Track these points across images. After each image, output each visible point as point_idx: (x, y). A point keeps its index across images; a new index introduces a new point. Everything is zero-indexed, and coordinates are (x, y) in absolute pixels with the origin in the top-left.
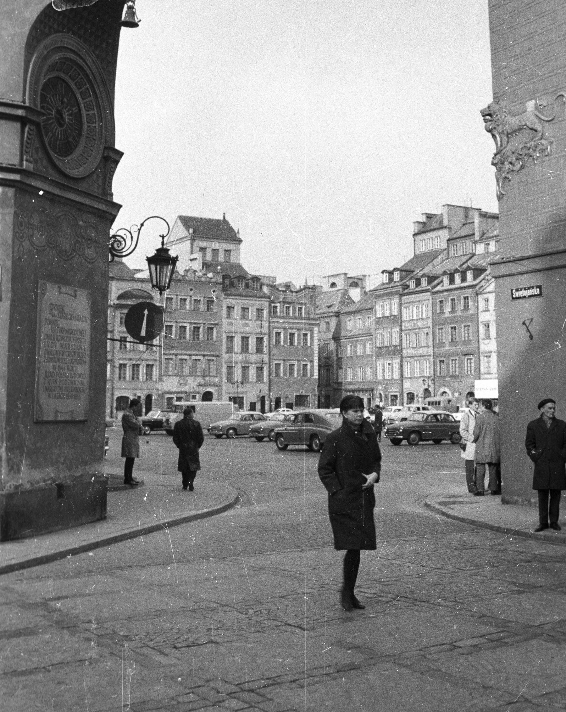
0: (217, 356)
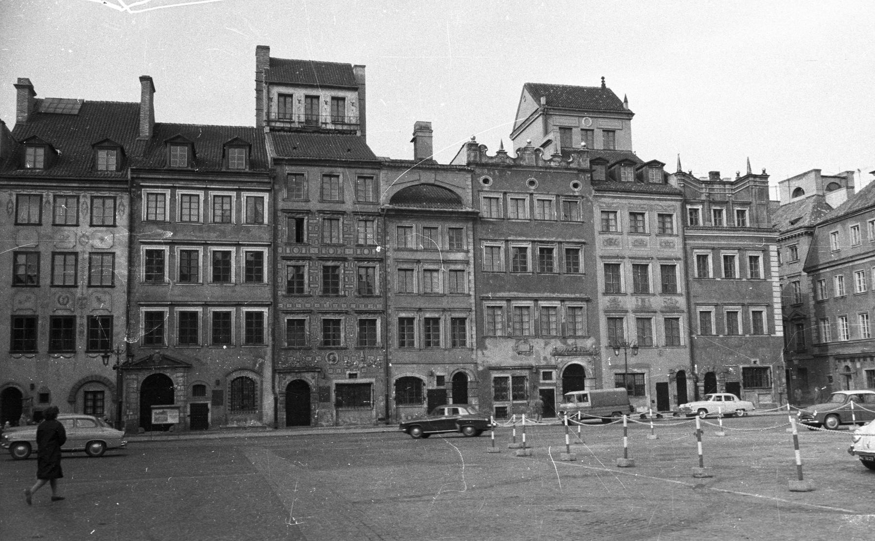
0: (588, 301)
